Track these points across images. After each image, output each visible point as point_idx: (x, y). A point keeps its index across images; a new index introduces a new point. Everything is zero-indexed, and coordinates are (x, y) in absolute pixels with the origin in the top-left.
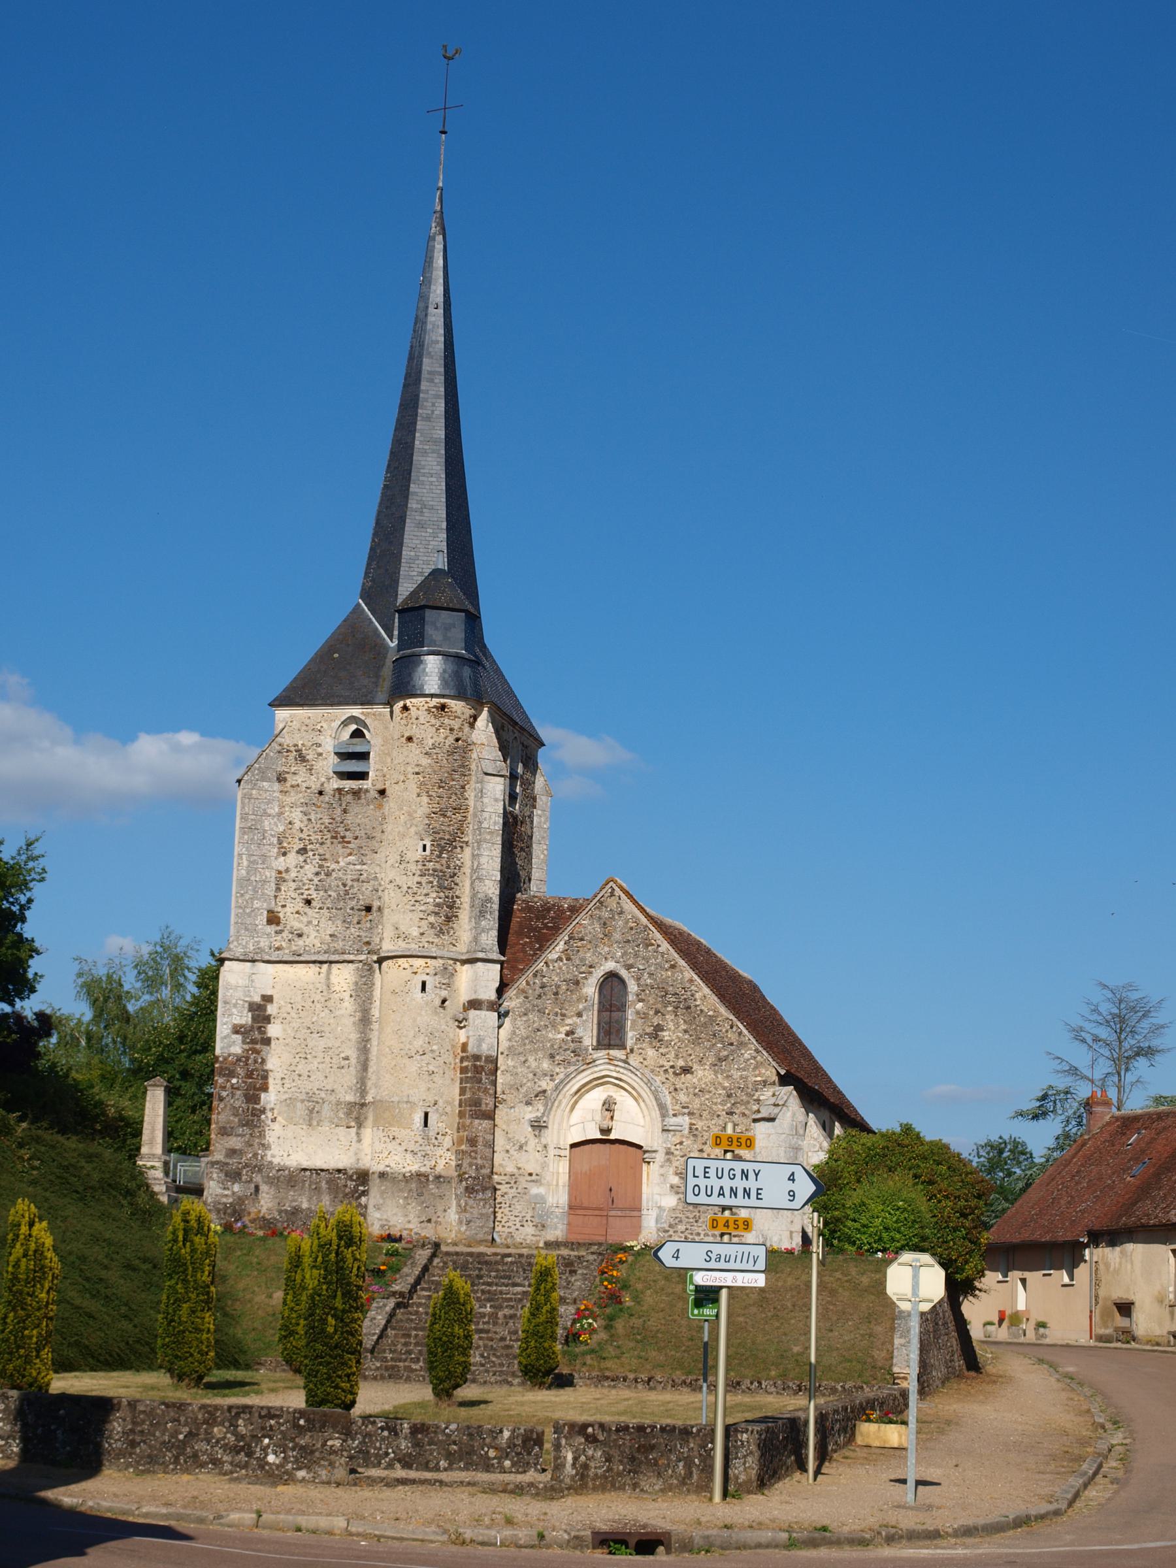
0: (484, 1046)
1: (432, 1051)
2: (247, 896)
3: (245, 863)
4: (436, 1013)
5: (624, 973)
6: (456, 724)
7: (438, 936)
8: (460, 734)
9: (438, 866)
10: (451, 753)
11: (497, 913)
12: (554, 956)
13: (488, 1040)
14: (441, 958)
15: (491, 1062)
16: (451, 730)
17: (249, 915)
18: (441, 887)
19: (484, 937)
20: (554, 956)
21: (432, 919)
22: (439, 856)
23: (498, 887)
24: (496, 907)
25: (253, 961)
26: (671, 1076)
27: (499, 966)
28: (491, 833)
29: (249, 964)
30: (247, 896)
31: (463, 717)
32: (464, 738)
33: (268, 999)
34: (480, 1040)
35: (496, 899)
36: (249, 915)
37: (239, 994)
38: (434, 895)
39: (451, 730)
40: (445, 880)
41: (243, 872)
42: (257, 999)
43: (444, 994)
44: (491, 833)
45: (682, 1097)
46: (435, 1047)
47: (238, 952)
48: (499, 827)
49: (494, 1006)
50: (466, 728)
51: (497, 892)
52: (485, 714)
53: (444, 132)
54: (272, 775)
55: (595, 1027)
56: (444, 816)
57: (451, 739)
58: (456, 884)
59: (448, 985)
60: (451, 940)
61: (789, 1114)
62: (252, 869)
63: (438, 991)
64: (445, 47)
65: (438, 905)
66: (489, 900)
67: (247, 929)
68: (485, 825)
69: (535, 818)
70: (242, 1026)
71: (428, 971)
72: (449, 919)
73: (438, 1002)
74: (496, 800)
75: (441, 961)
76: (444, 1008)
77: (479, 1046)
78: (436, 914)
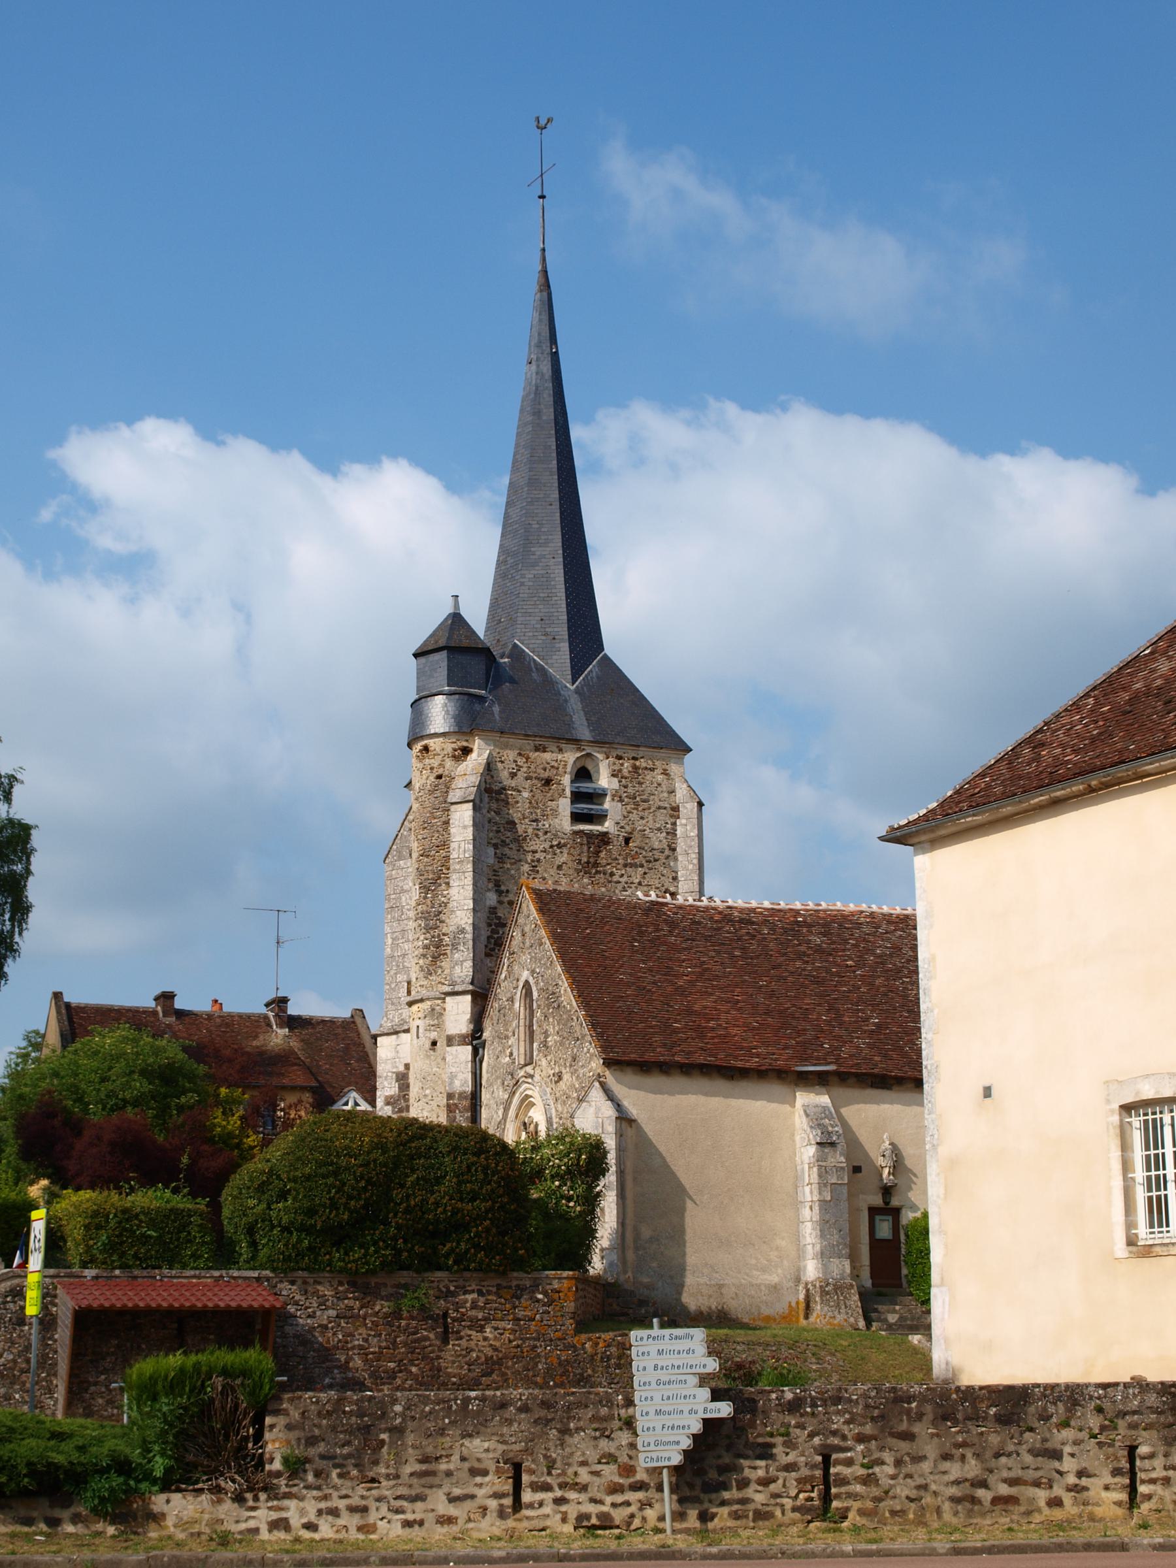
0: (457, 1083)
1: (425, 1096)
2: (392, 972)
3: (390, 941)
4: (428, 1057)
5: (531, 981)
6: (435, 762)
7: (426, 978)
8: (440, 771)
9: (425, 908)
10: (431, 792)
11: (471, 943)
12: (503, 976)
13: (461, 1076)
14: (428, 999)
15: (466, 1098)
16: (432, 769)
17: (394, 990)
18: (428, 929)
19: (458, 969)
20: (503, 976)
21: (421, 962)
22: (425, 898)
23: (470, 915)
24: (469, 936)
25: (396, 1033)
26: (553, 1086)
27: (469, 998)
28: (461, 862)
29: (394, 1037)
30: (392, 972)
31: (442, 754)
32: (446, 773)
33: (407, 1066)
34: (453, 1077)
35: (469, 929)
36: (394, 990)
37: (389, 1067)
38: (422, 938)
39: (432, 769)
40: (432, 917)
41: (389, 950)
42: (402, 1068)
43: (434, 1035)
44: (461, 862)
45: (560, 1108)
46: (428, 1092)
47: (388, 1026)
48: (469, 854)
49: (463, 1040)
50: (449, 763)
51: (470, 921)
52: (477, 744)
53: (542, 197)
54: (405, 853)
55: (522, 1043)
56: (428, 856)
57: (432, 778)
58: (442, 922)
59: (438, 1026)
60: (439, 979)
61: (592, 1110)
62: (395, 946)
63: (428, 1034)
64: (538, 119)
65: (426, 947)
66: (463, 931)
67: (393, 1004)
68: (454, 855)
69: (679, 828)
70: (392, 1097)
71: (420, 1015)
72: (435, 958)
73: (428, 1045)
74: (465, 827)
75: (429, 1003)
76: (434, 1050)
77: (451, 1083)
78: (424, 956)
